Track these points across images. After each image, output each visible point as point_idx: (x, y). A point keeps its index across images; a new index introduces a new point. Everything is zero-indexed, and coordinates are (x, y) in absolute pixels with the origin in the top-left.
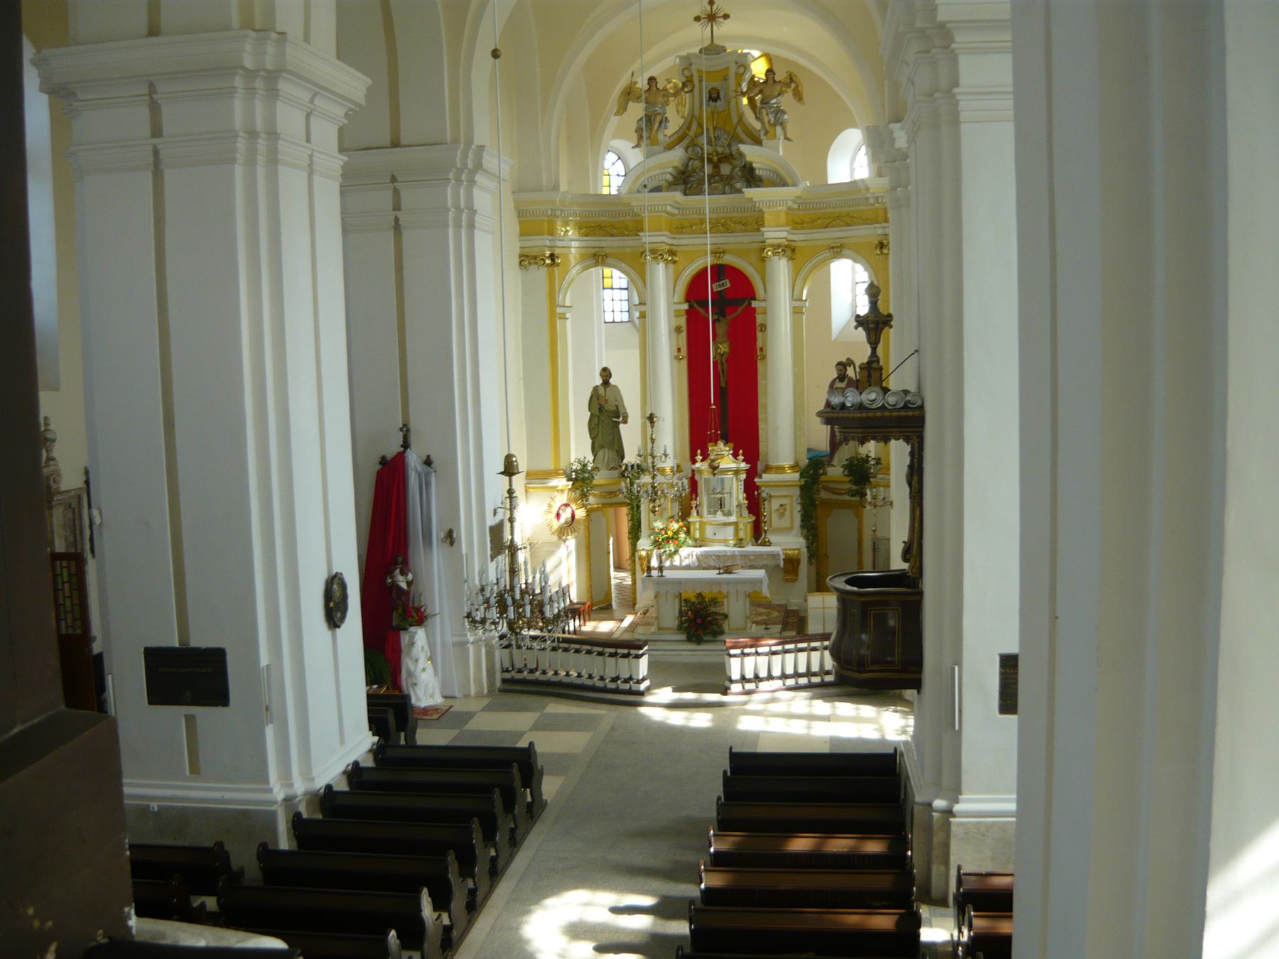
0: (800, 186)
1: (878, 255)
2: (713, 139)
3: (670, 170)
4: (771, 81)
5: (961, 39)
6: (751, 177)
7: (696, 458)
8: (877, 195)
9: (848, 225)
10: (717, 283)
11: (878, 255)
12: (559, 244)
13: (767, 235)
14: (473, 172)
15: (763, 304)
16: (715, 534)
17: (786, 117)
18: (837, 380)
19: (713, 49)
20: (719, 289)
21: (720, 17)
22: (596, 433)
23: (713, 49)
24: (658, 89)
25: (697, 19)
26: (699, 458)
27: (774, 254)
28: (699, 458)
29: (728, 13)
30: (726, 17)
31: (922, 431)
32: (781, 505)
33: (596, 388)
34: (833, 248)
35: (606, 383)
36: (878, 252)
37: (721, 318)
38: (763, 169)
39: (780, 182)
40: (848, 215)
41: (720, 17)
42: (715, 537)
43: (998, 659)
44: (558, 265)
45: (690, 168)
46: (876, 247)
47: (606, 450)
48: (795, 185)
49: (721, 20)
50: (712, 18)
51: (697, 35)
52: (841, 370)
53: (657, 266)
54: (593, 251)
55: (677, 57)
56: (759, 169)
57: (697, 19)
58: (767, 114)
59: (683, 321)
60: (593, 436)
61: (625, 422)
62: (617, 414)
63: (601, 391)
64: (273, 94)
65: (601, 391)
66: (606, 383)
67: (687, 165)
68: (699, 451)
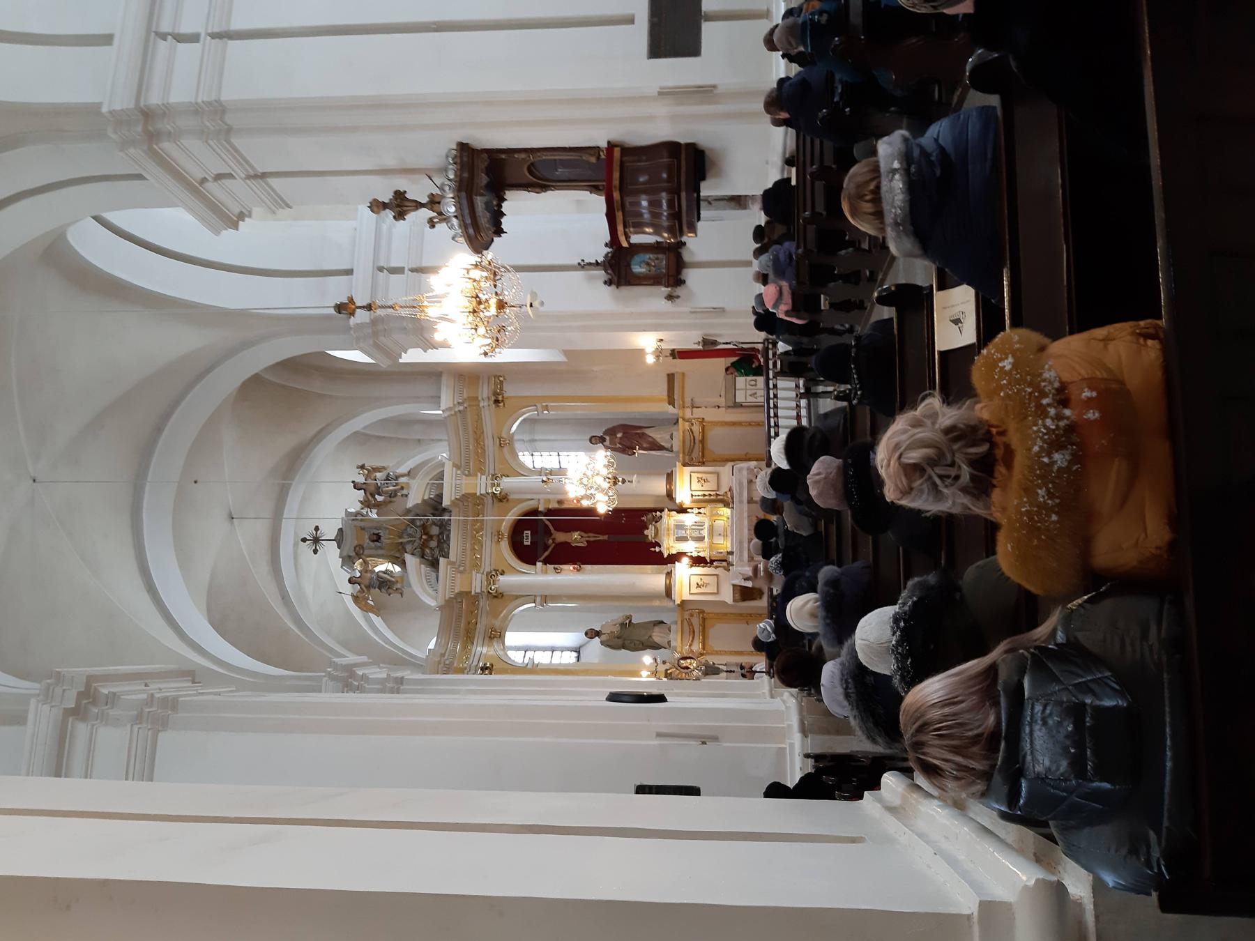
0: (444, 460)
1: (504, 405)
2: (409, 539)
3: (423, 566)
4: (364, 486)
5: (154, 98)
6: (435, 506)
7: (657, 551)
8: (456, 403)
9: (483, 432)
10: (525, 540)
11: (504, 405)
12: (475, 663)
13: (483, 492)
14: (352, 675)
15: (542, 502)
16: (720, 535)
17: (391, 473)
18: (605, 443)
19: (340, 539)
20: (529, 540)
21: (316, 533)
22: (638, 642)
23: (340, 539)
24: (360, 577)
25: (315, 552)
26: (657, 549)
27: (499, 485)
28: (657, 549)
29: (314, 527)
30: (317, 529)
31: (477, 150)
32: (699, 481)
33: (602, 643)
34: (500, 444)
35: (598, 634)
36: (501, 404)
37: (552, 537)
38: (431, 489)
39: (441, 476)
40: (475, 432)
41: (316, 533)
42: (722, 534)
43: (653, 61)
44: (492, 665)
45: (430, 558)
46: (499, 406)
47: (654, 634)
48: (443, 465)
49: (319, 532)
50: (316, 540)
51: (331, 552)
52: (596, 439)
53: (500, 581)
54: (487, 639)
55: (342, 567)
56: (430, 494)
57: (315, 552)
58: (387, 487)
59: (550, 567)
60: (641, 646)
61: (629, 617)
62: (623, 625)
63: (604, 637)
64: (113, 699)
65: (604, 637)
66: (598, 634)
67: (428, 560)
68: (653, 549)
